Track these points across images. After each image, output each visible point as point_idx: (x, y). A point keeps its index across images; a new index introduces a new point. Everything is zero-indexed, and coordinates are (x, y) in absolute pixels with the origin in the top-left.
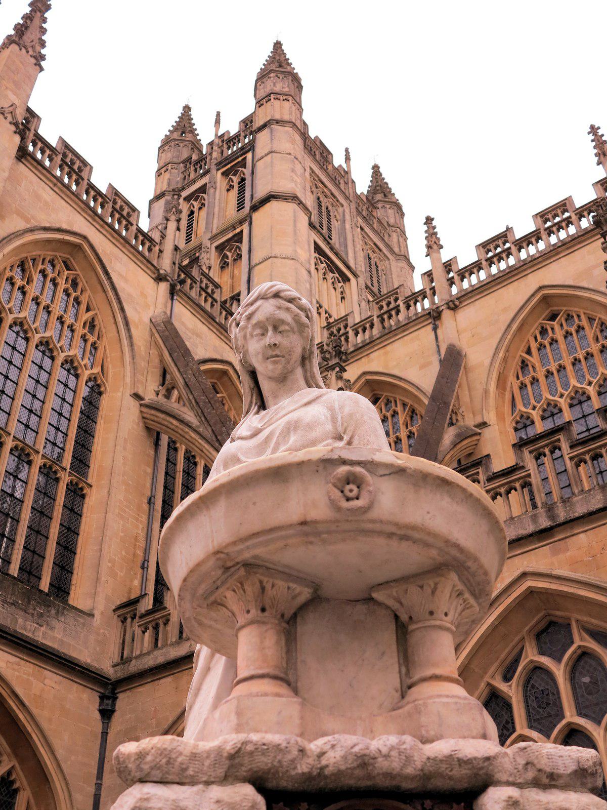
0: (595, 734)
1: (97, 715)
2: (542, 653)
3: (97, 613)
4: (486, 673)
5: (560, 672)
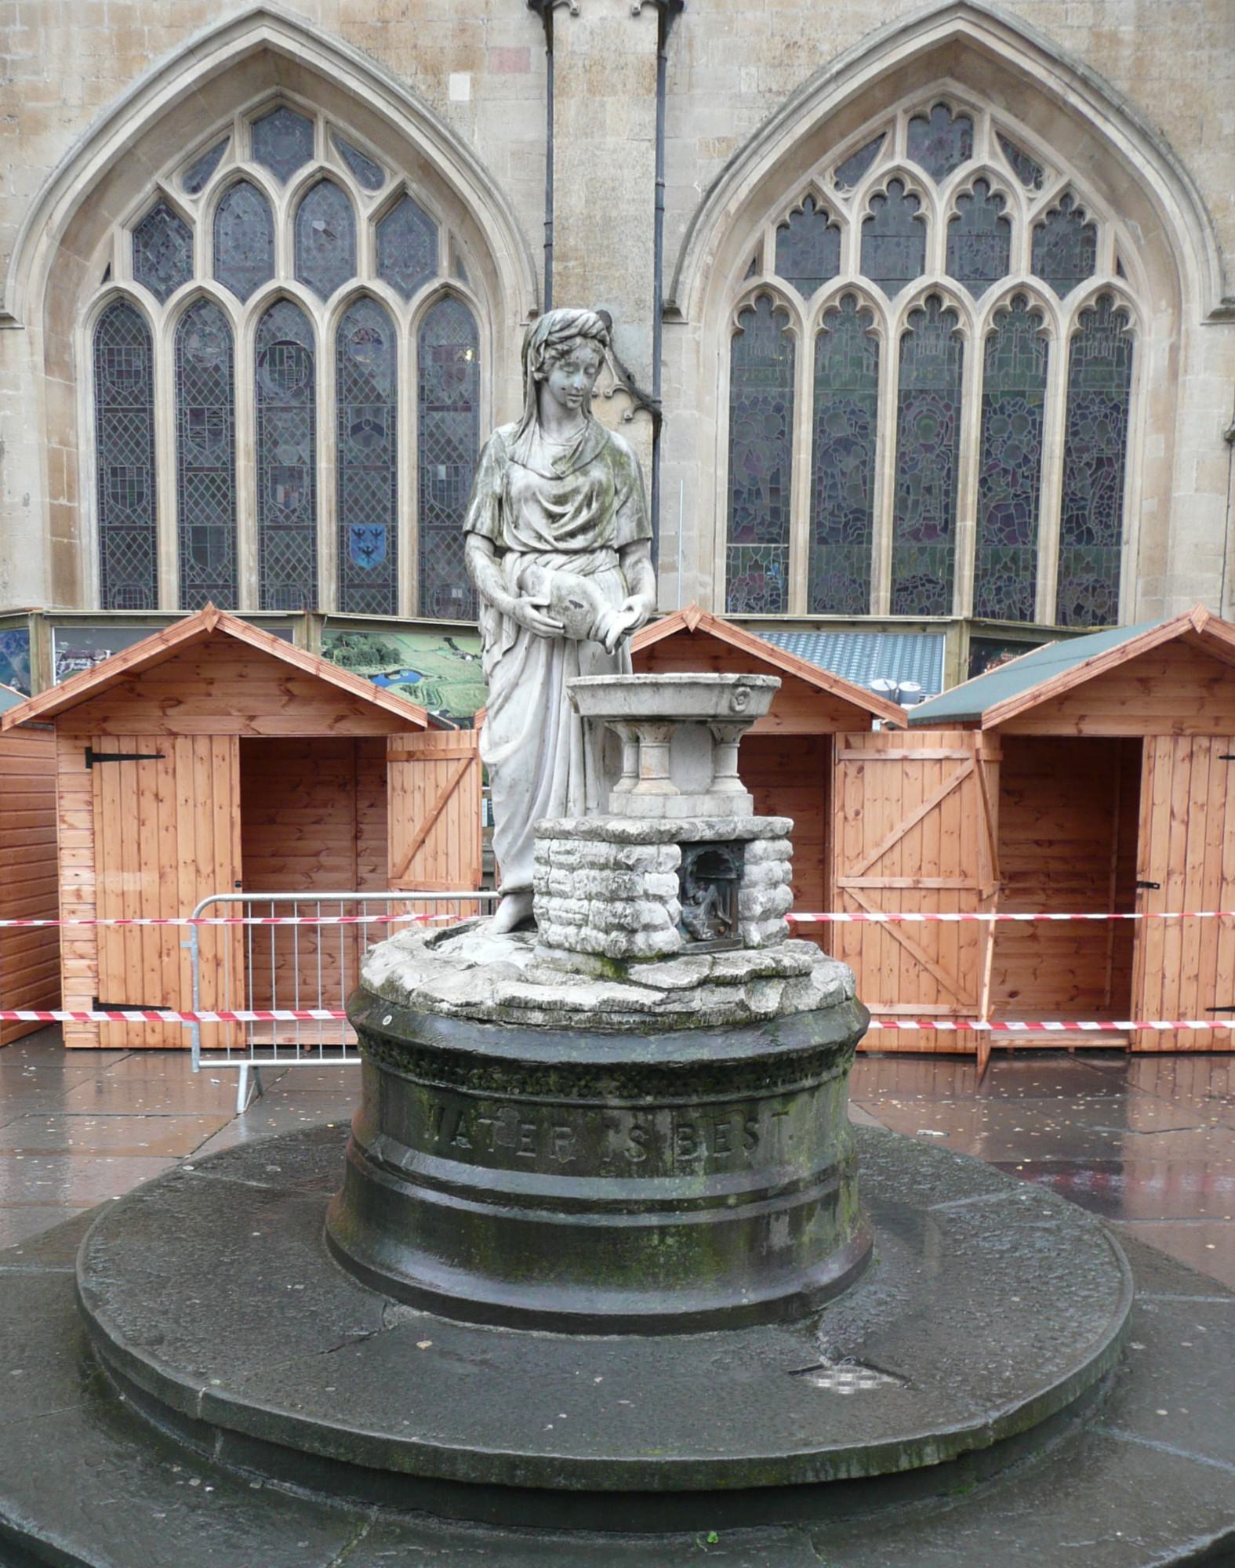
0: (316, 314)
2: (258, 157)
4: (157, 168)
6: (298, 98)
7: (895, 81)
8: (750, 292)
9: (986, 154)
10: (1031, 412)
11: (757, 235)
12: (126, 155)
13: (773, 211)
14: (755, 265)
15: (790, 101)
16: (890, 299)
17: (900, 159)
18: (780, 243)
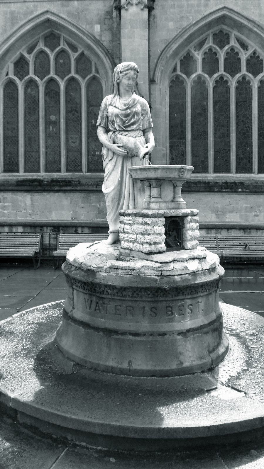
0: (61, 83)
2: (46, 45)
4: (20, 48)
5: (52, 57)
6: (56, 31)
7: (209, 25)
8: (173, 77)
9: (233, 43)
10: (249, 106)
11: (175, 62)
12: (13, 45)
13: (179, 56)
14: (175, 70)
15: (182, 30)
16: (210, 78)
17: (211, 44)
18: (181, 64)
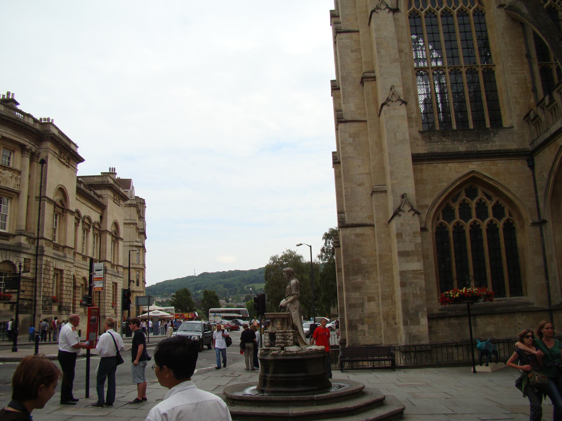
1: (528, 168)
3: (514, 125)
